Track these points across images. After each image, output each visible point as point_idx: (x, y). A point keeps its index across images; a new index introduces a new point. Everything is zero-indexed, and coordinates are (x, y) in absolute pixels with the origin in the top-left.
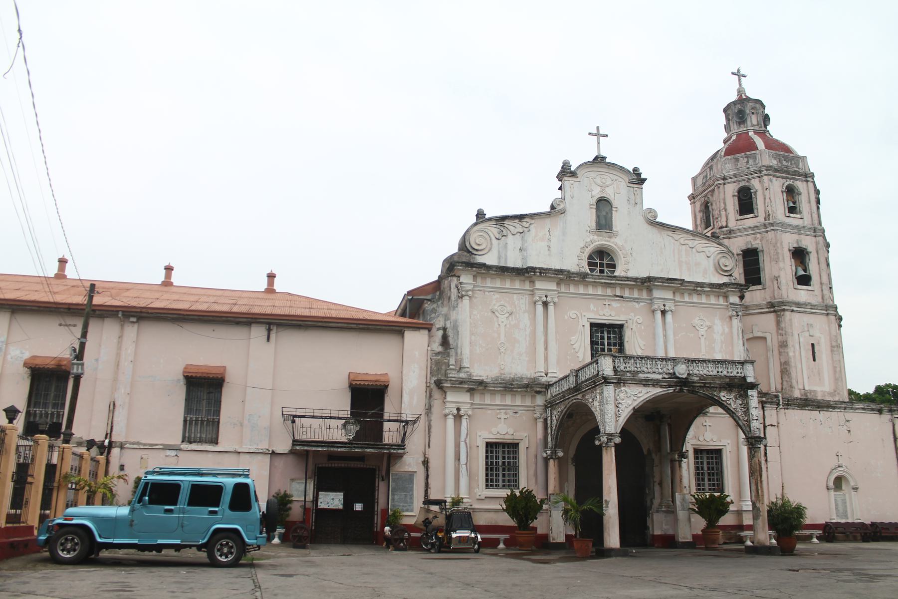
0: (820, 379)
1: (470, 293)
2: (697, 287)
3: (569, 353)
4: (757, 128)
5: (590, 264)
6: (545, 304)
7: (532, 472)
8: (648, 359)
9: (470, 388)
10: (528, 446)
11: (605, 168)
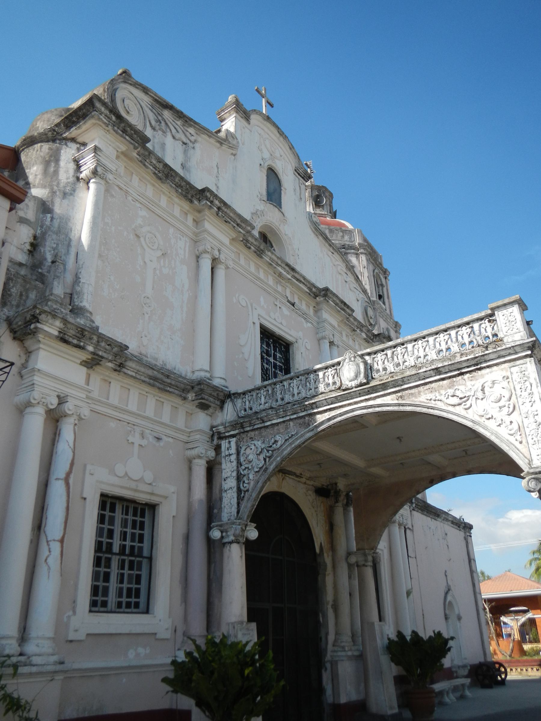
1: (110, 176)
2: (358, 328)
3: (237, 357)
10: (174, 514)
11: (276, 136)
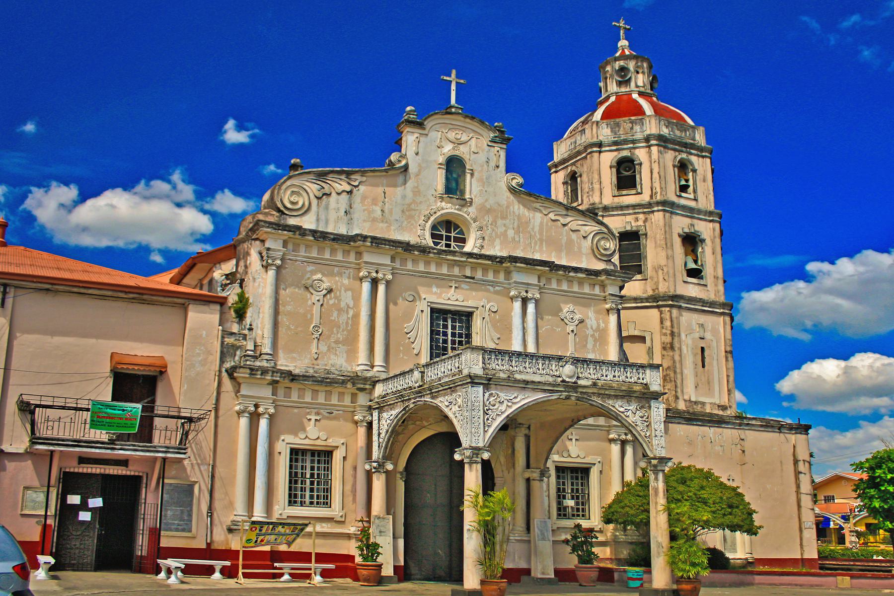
0: (709, 389)
4: (642, 89)
5: (433, 236)
6: (375, 282)
7: (348, 487)
8: (500, 353)
9: (274, 381)
